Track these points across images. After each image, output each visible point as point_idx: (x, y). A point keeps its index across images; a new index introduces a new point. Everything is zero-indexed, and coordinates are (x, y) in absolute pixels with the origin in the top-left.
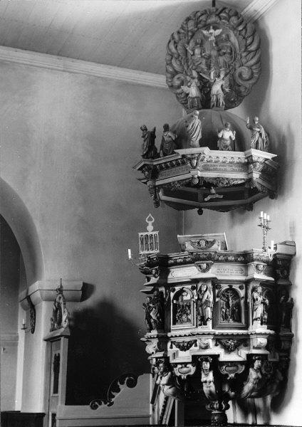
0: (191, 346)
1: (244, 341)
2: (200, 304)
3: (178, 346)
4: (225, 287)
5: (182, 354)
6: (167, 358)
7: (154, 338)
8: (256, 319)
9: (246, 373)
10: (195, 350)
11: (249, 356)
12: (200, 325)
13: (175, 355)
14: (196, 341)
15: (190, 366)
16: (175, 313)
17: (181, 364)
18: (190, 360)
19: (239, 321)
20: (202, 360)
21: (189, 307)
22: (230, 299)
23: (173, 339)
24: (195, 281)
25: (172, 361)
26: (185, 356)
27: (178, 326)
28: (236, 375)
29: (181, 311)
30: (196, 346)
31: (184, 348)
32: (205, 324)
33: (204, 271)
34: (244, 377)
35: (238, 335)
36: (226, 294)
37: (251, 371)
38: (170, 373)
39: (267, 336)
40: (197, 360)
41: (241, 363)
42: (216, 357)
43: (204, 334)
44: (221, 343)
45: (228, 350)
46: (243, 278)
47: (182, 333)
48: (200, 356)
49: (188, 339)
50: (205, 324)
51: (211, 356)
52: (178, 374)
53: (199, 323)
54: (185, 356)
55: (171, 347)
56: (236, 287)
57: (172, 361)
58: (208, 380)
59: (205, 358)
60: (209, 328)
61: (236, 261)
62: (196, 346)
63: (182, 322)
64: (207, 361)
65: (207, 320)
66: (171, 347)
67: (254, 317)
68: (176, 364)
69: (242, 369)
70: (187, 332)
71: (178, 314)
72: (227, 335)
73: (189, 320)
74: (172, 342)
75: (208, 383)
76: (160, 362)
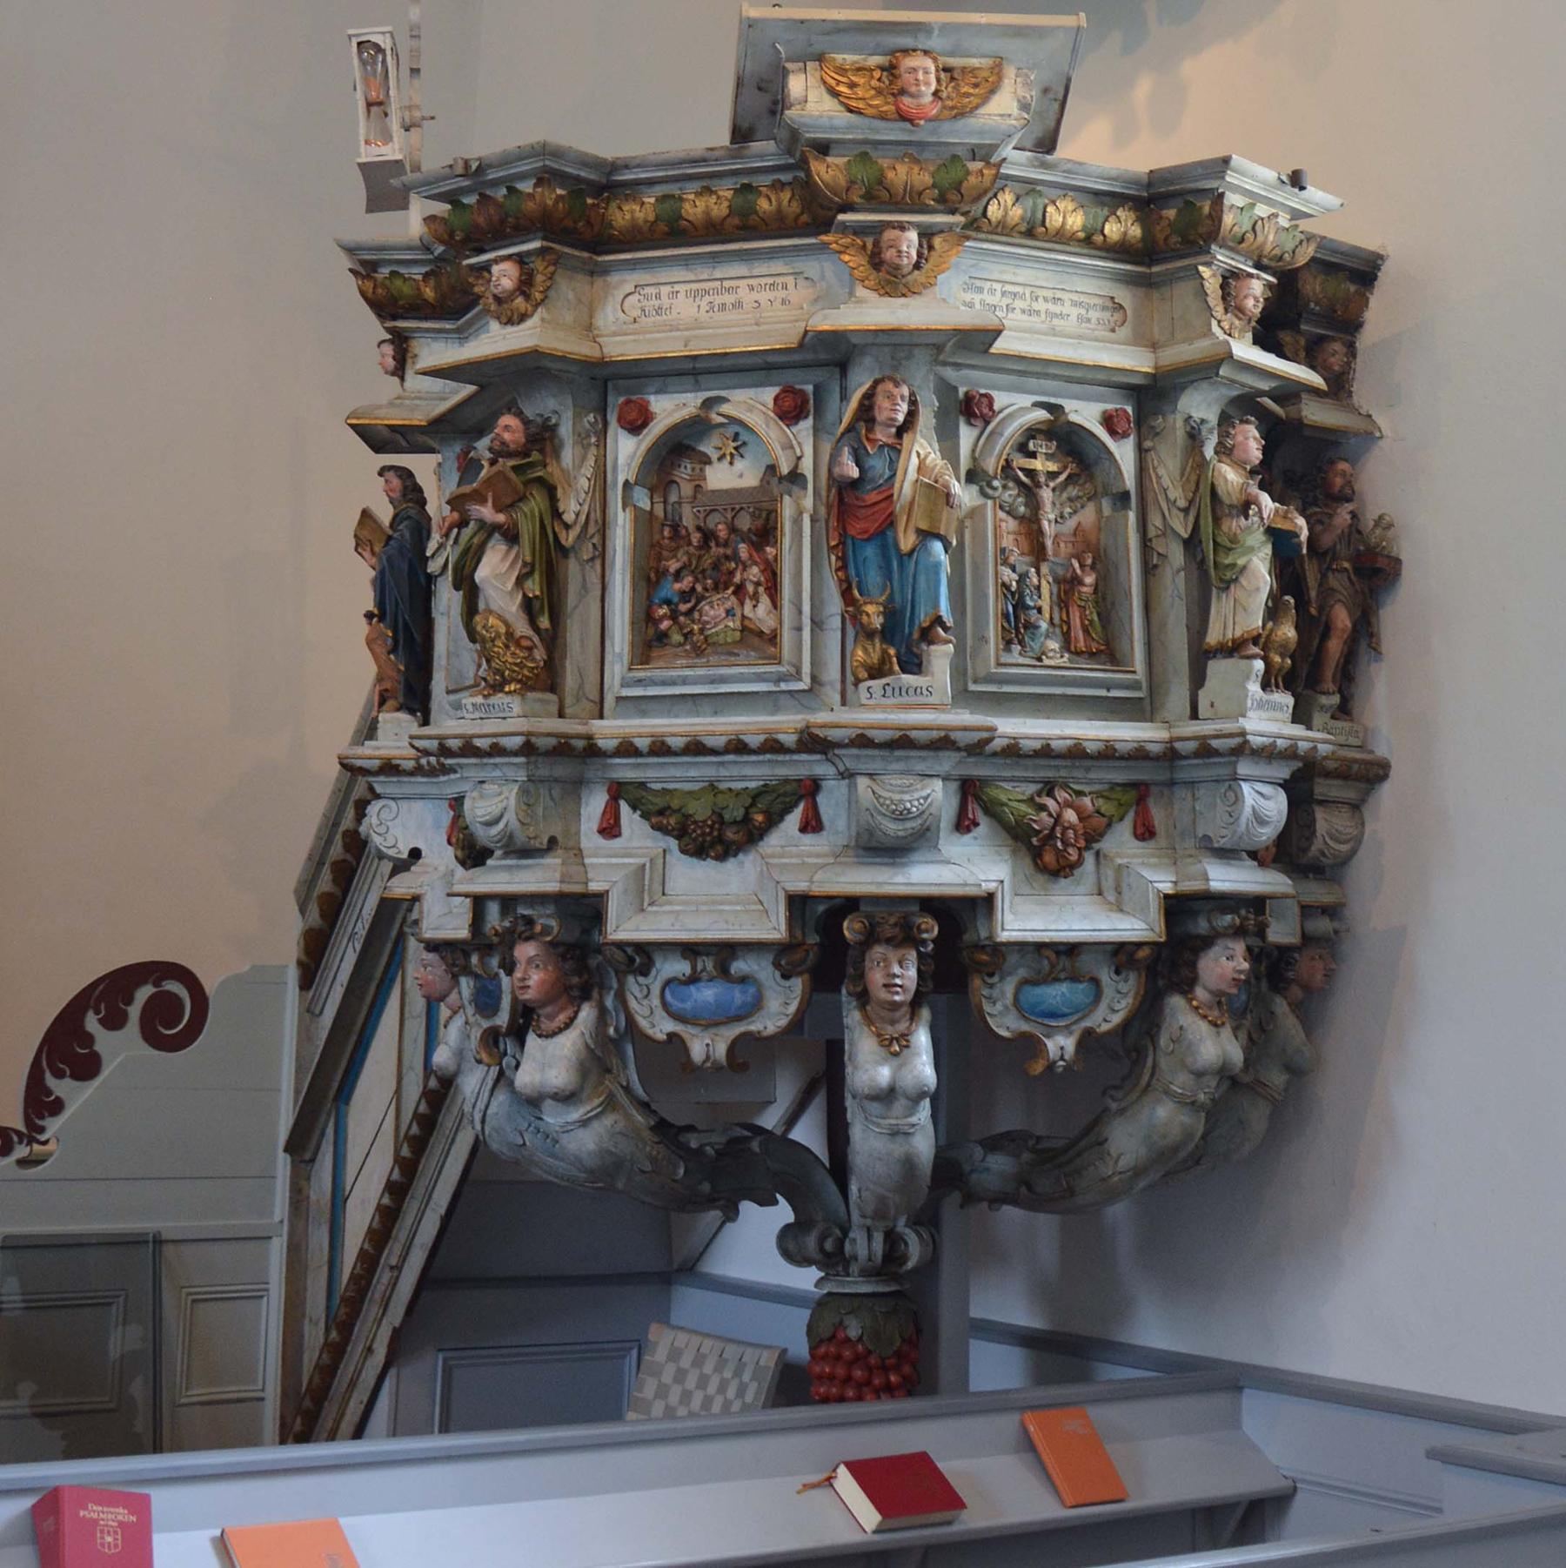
0: (774, 820)
1: (1145, 789)
2: (858, 514)
3: (666, 816)
4: (1018, 407)
5: (691, 876)
6: (585, 910)
7: (497, 750)
8: (1234, 649)
9: (1146, 1019)
10: (799, 860)
11: (1177, 907)
12: (876, 672)
13: (647, 887)
14: (811, 788)
15: (760, 968)
16: (648, 578)
17: (690, 950)
18: (774, 927)
19: (1109, 653)
20: (871, 937)
21: (766, 533)
22: (1046, 495)
23: (625, 770)
24: (833, 354)
25: (623, 926)
26: (730, 899)
27: (682, 674)
28: (1088, 1040)
29: (701, 564)
30: (812, 824)
31: (717, 834)
32: (914, 664)
33: (890, 279)
34: (1126, 1055)
35: (1108, 753)
36: (1020, 461)
37: (1181, 1015)
38: (587, 1013)
39: (1283, 771)
40: (827, 942)
41: (1121, 954)
42: (960, 914)
43: (862, 741)
44: (992, 810)
45: (1047, 856)
46: (1137, 361)
47: (677, 726)
48: (850, 904)
49: (750, 774)
50: (914, 664)
51: (932, 905)
52: (661, 1027)
53: (872, 652)
54: (730, 899)
55: (610, 828)
56: (1085, 413)
57: (623, 926)
58: (908, 1081)
59: (899, 919)
60: (929, 699)
61: (1089, 241)
62: (812, 824)
63: (701, 646)
64: (907, 937)
65: (927, 635)
66: (610, 828)
67: (1213, 637)
68: (641, 956)
69: (1110, 1014)
70: (787, 723)
71: (672, 588)
72: (1045, 752)
73: (762, 641)
74: (617, 791)
75: (900, 1105)
76: (524, 930)
